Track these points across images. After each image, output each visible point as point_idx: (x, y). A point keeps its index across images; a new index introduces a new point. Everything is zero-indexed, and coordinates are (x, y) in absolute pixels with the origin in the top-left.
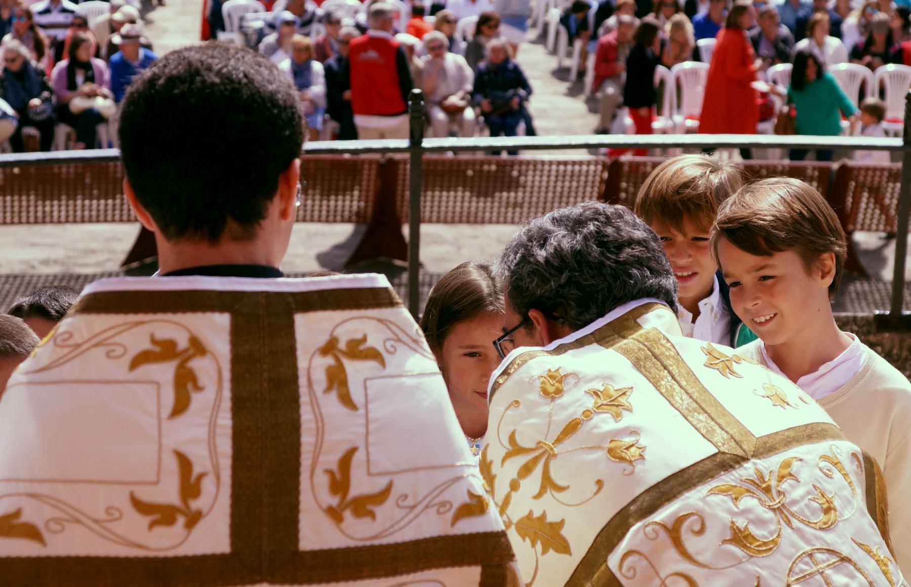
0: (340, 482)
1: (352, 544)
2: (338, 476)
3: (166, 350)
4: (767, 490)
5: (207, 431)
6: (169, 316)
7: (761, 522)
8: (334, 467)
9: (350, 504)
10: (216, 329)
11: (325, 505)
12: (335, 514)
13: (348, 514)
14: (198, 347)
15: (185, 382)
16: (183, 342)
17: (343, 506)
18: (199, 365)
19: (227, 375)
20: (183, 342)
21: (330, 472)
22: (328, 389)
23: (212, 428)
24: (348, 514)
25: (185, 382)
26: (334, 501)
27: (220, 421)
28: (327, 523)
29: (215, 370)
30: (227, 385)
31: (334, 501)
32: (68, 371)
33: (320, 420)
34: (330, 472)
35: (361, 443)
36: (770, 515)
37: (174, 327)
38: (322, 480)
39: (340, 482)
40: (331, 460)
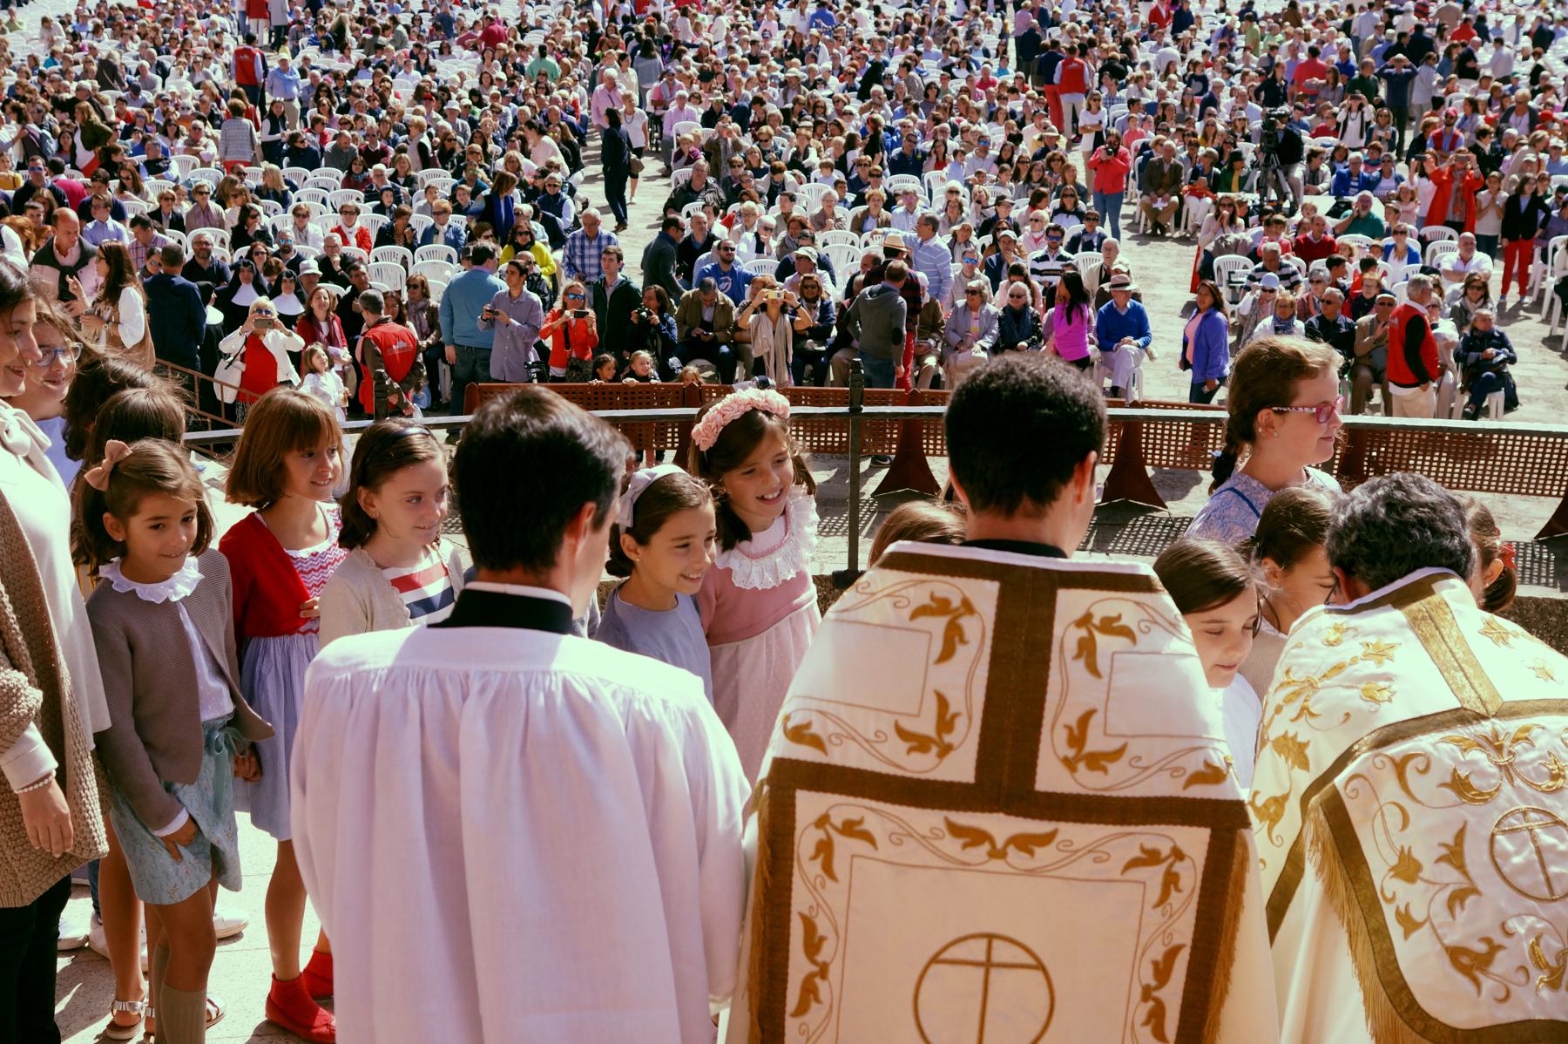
0: (1077, 737)
1: (1083, 791)
2: (1076, 732)
4: (1499, 749)
5: (967, 680)
7: (1483, 774)
8: (1074, 723)
9: (1081, 755)
10: (985, 594)
11: (1061, 755)
12: (1070, 764)
14: (968, 607)
16: (956, 602)
17: (1077, 759)
18: (967, 623)
19: (990, 634)
20: (956, 602)
21: (1069, 728)
22: (1078, 656)
23: (971, 676)
26: (1071, 753)
27: (978, 672)
28: (1063, 771)
29: (980, 628)
31: (1071, 753)
33: (1065, 682)
34: (1069, 728)
36: (1494, 770)
37: (951, 588)
39: (1077, 737)
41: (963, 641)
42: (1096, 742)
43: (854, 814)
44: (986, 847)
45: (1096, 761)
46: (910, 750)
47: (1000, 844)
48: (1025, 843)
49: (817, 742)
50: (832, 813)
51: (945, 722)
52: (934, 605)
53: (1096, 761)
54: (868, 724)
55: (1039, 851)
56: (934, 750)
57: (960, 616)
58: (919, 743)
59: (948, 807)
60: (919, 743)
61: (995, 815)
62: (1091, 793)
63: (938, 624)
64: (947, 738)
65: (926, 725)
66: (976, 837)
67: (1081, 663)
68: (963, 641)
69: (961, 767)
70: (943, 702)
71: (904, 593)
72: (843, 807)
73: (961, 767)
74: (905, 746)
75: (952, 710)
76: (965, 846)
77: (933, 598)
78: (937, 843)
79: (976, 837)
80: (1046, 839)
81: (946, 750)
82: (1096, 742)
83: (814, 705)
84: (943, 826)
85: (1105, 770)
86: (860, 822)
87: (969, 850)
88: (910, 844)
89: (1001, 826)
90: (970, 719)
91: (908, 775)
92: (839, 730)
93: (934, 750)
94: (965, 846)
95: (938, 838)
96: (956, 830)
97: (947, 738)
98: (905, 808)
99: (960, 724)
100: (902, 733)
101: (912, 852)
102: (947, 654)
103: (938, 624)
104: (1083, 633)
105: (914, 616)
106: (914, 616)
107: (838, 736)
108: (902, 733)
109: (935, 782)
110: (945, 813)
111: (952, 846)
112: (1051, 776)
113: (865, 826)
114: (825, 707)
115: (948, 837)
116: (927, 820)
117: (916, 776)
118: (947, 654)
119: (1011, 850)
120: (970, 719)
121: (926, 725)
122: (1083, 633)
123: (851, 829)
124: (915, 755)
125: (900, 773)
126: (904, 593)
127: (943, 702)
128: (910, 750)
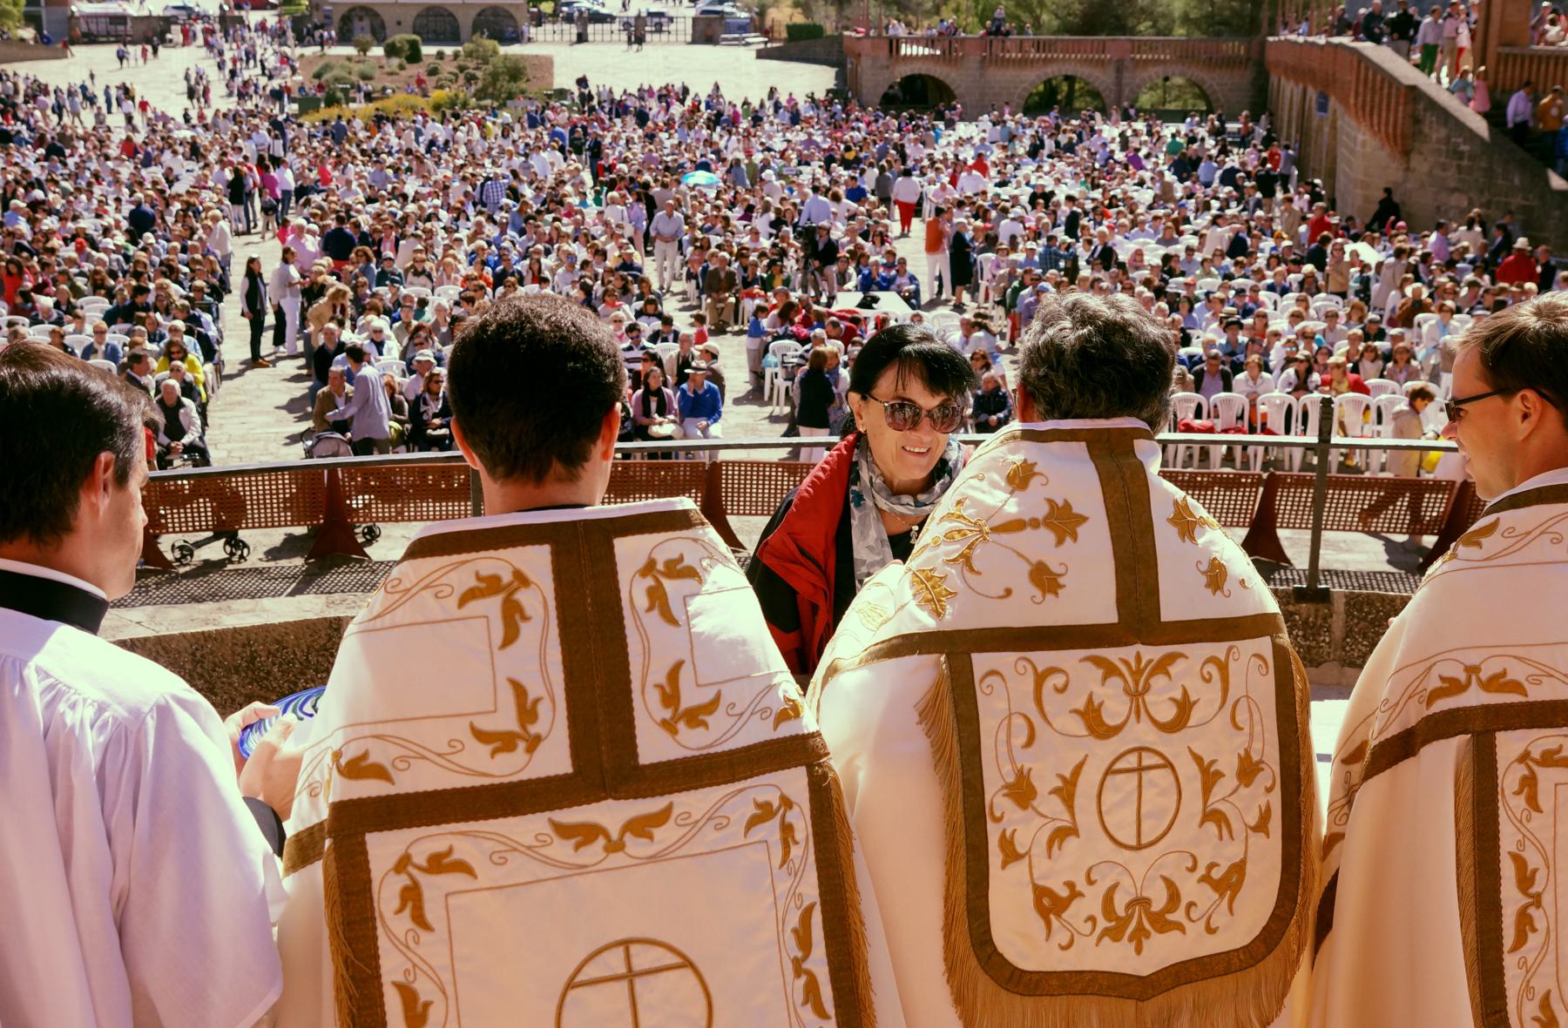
0: (670, 696)
2: (668, 690)
3: (490, 585)
5: (539, 658)
6: (492, 553)
10: (537, 560)
12: (669, 726)
13: (681, 726)
14: (521, 579)
15: (513, 616)
16: (507, 577)
17: (676, 718)
18: (522, 596)
19: (552, 604)
20: (507, 577)
21: (660, 687)
22: (650, 609)
24: (681, 726)
25: (513, 616)
26: (667, 714)
28: (664, 735)
29: (540, 599)
30: (553, 614)
31: (667, 714)
32: (400, 616)
35: (686, 656)
38: (654, 697)
39: (670, 696)
40: (659, 675)
41: (525, 618)
42: (691, 697)
43: (440, 846)
44: (601, 841)
45: (695, 717)
46: (493, 753)
47: (615, 835)
48: (641, 827)
49: (380, 772)
50: (411, 851)
51: (527, 712)
52: (483, 585)
53: (695, 717)
54: (435, 736)
55: (658, 833)
56: (522, 745)
57: (516, 589)
58: (503, 742)
59: (550, 808)
60: (503, 742)
61: (603, 803)
62: (697, 753)
63: (492, 606)
64: (534, 729)
65: (507, 720)
66: (587, 834)
67: (656, 613)
68: (525, 618)
69: (555, 759)
70: (519, 690)
71: (444, 580)
72: (425, 841)
73: (555, 759)
74: (486, 749)
75: (531, 697)
76: (577, 847)
77: (478, 577)
78: (544, 851)
79: (587, 834)
80: (662, 817)
81: (534, 743)
82: (691, 697)
83: (367, 730)
84: (548, 830)
85: (705, 724)
86: (450, 851)
87: (582, 850)
88: (516, 860)
89: (610, 814)
90: (553, 702)
91: (496, 781)
92: (403, 752)
93: (522, 745)
94: (577, 847)
95: (545, 844)
96: (563, 831)
97: (534, 729)
98: (501, 820)
99: (544, 710)
100: (481, 736)
101: (520, 868)
102: (510, 637)
103: (492, 606)
104: (649, 581)
105: (463, 602)
106: (463, 602)
107: (402, 758)
108: (481, 736)
109: (530, 781)
110: (548, 814)
111: (562, 850)
112: (654, 746)
113: (455, 856)
114: (380, 729)
115: (557, 840)
116: (528, 827)
117: (506, 780)
118: (510, 637)
119: (628, 838)
120: (553, 702)
121: (507, 720)
122: (649, 581)
123: (439, 864)
124: (502, 757)
125: (487, 781)
126: (444, 580)
127: (519, 690)
128: (493, 753)
